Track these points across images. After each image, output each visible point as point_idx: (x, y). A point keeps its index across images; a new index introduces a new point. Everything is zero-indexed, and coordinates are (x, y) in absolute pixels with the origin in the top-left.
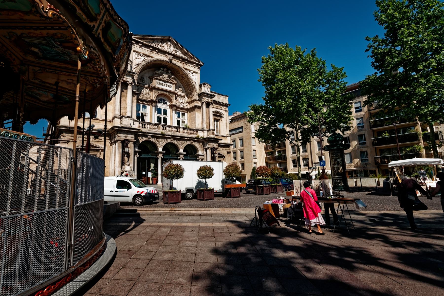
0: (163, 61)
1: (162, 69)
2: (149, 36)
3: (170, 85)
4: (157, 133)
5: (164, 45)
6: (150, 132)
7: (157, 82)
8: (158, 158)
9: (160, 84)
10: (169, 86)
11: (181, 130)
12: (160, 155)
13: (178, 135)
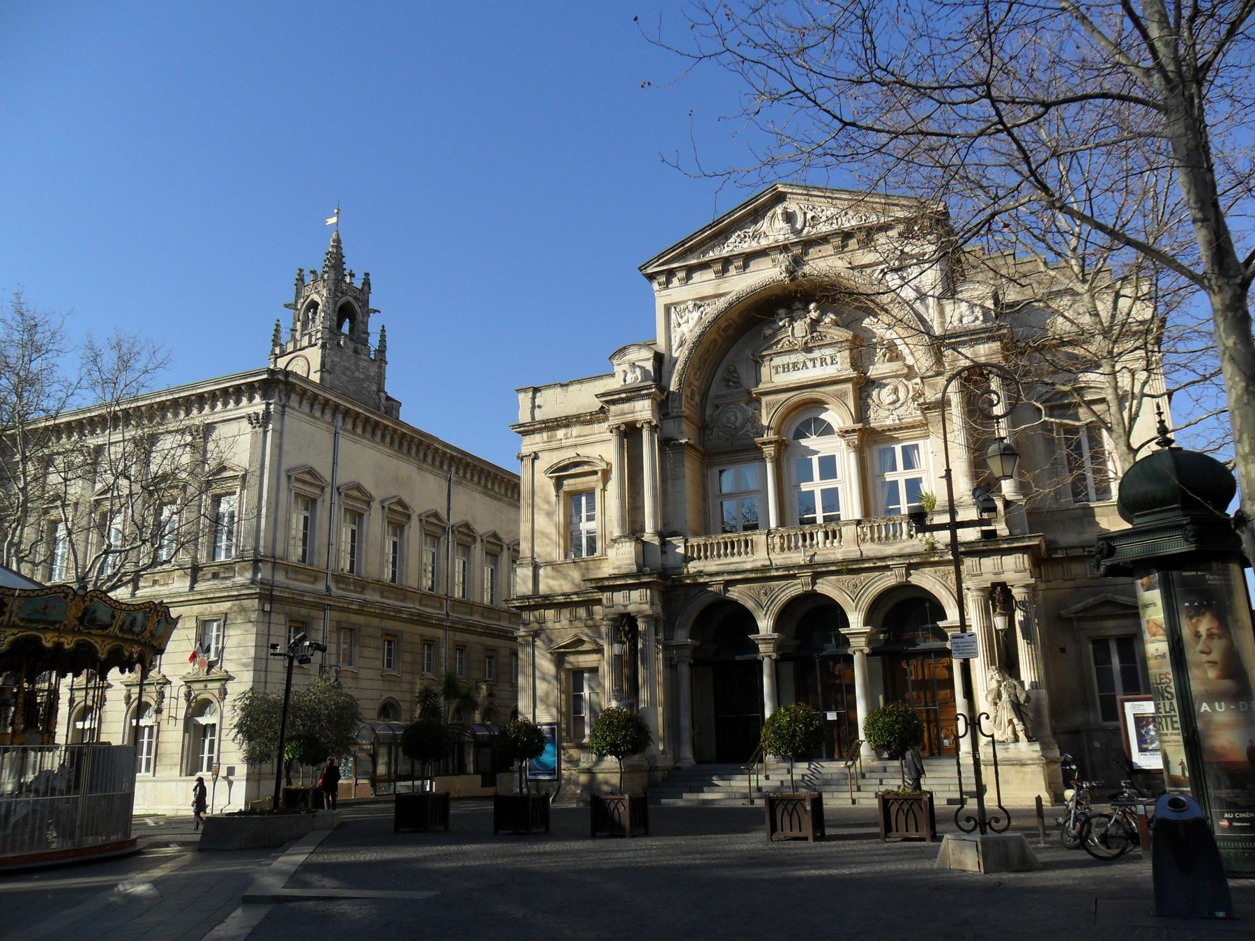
0: (765, 288)
1: (782, 312)
2: (703, 231)
3: (828, 352)
4: (749, 566)
5: (764, 225)
6: (722, 568)
7: (777, 368)
8: (761, 663)
9: (786, 368)
10: (823, 361)
11: (849, 532)
12: (762, 648)
13: (832, 557)
